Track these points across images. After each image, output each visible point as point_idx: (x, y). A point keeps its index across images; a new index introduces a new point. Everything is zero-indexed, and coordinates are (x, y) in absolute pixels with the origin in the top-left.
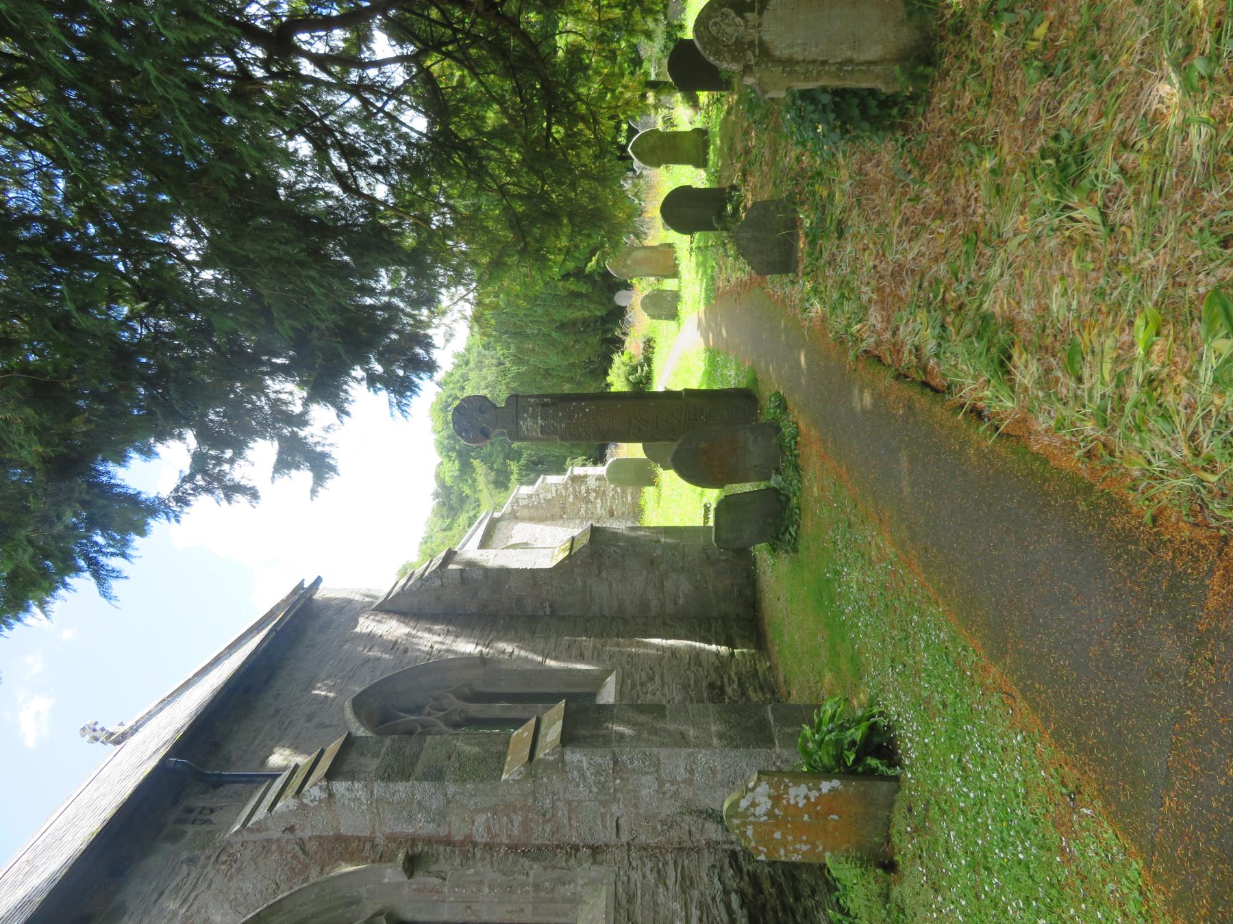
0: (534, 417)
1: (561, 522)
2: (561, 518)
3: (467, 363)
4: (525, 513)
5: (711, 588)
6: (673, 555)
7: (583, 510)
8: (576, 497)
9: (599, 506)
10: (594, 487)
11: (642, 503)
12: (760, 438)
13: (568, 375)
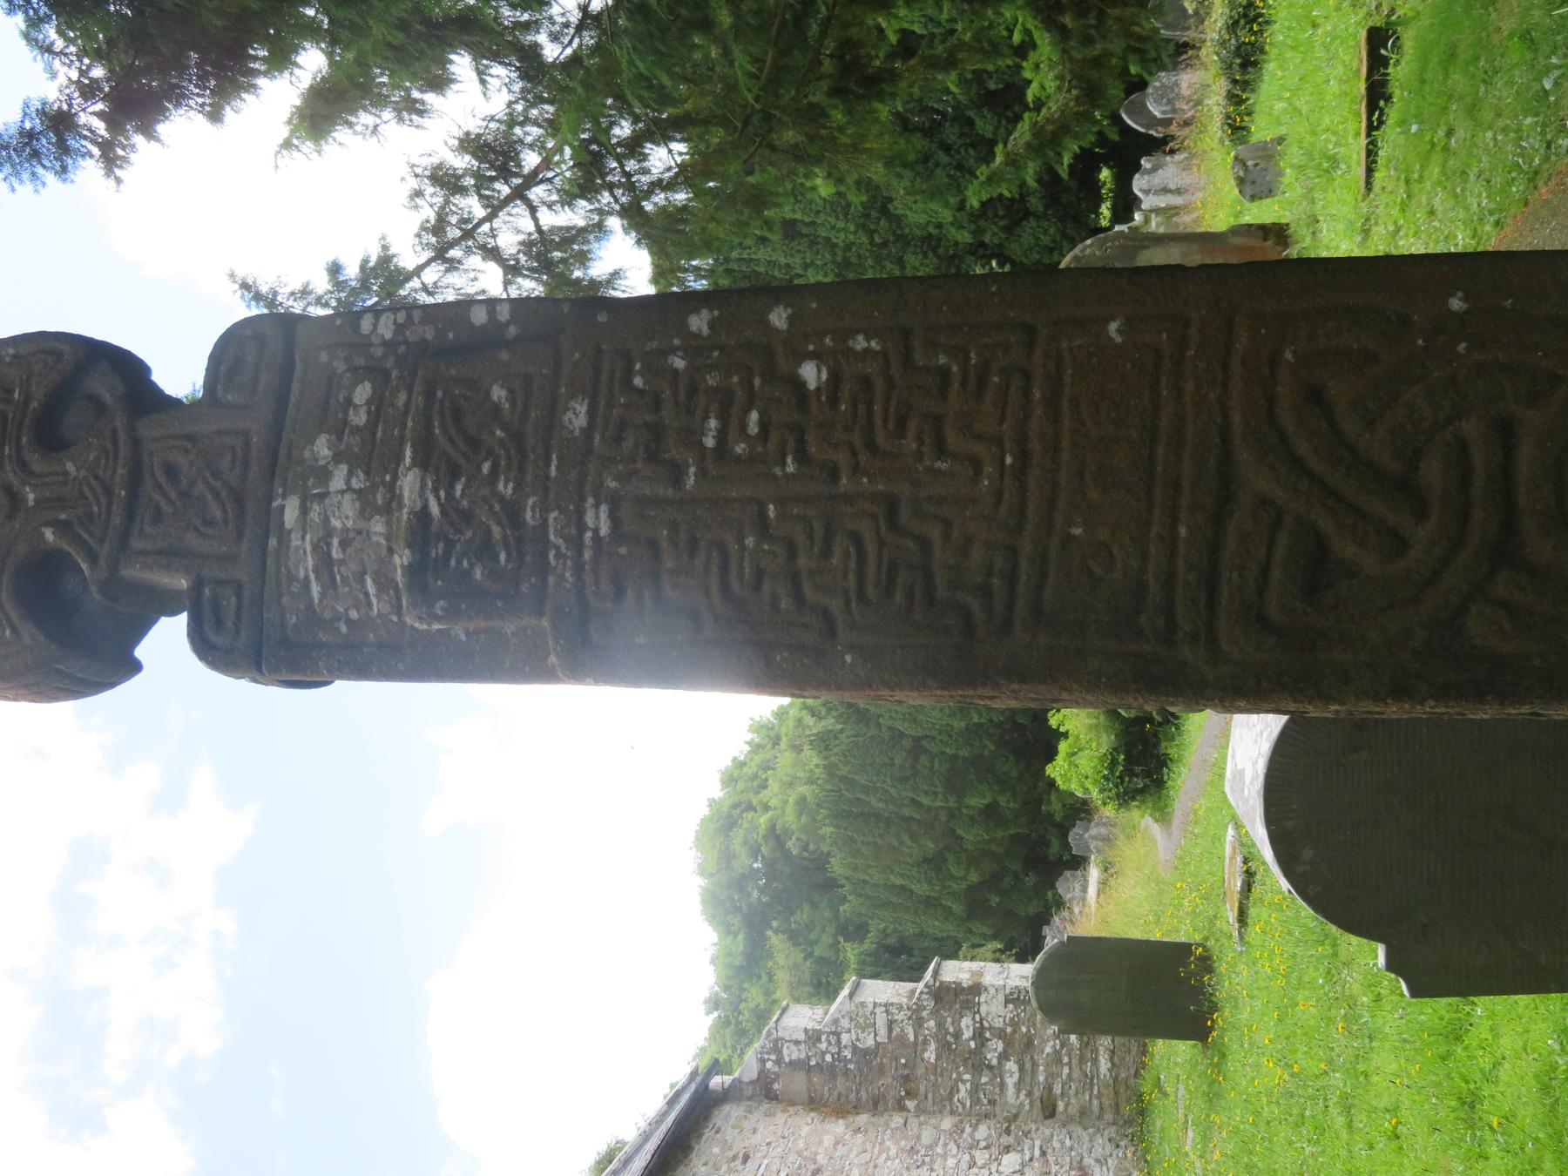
1: (898, 1120)
2: (902, 1108)
3: (776, 741)
4: (798, 1083)
7: (964, 1090)
8: (944, 1047)
9: (1011, 1082)
10: (998, 1023)
13: (964, 753)
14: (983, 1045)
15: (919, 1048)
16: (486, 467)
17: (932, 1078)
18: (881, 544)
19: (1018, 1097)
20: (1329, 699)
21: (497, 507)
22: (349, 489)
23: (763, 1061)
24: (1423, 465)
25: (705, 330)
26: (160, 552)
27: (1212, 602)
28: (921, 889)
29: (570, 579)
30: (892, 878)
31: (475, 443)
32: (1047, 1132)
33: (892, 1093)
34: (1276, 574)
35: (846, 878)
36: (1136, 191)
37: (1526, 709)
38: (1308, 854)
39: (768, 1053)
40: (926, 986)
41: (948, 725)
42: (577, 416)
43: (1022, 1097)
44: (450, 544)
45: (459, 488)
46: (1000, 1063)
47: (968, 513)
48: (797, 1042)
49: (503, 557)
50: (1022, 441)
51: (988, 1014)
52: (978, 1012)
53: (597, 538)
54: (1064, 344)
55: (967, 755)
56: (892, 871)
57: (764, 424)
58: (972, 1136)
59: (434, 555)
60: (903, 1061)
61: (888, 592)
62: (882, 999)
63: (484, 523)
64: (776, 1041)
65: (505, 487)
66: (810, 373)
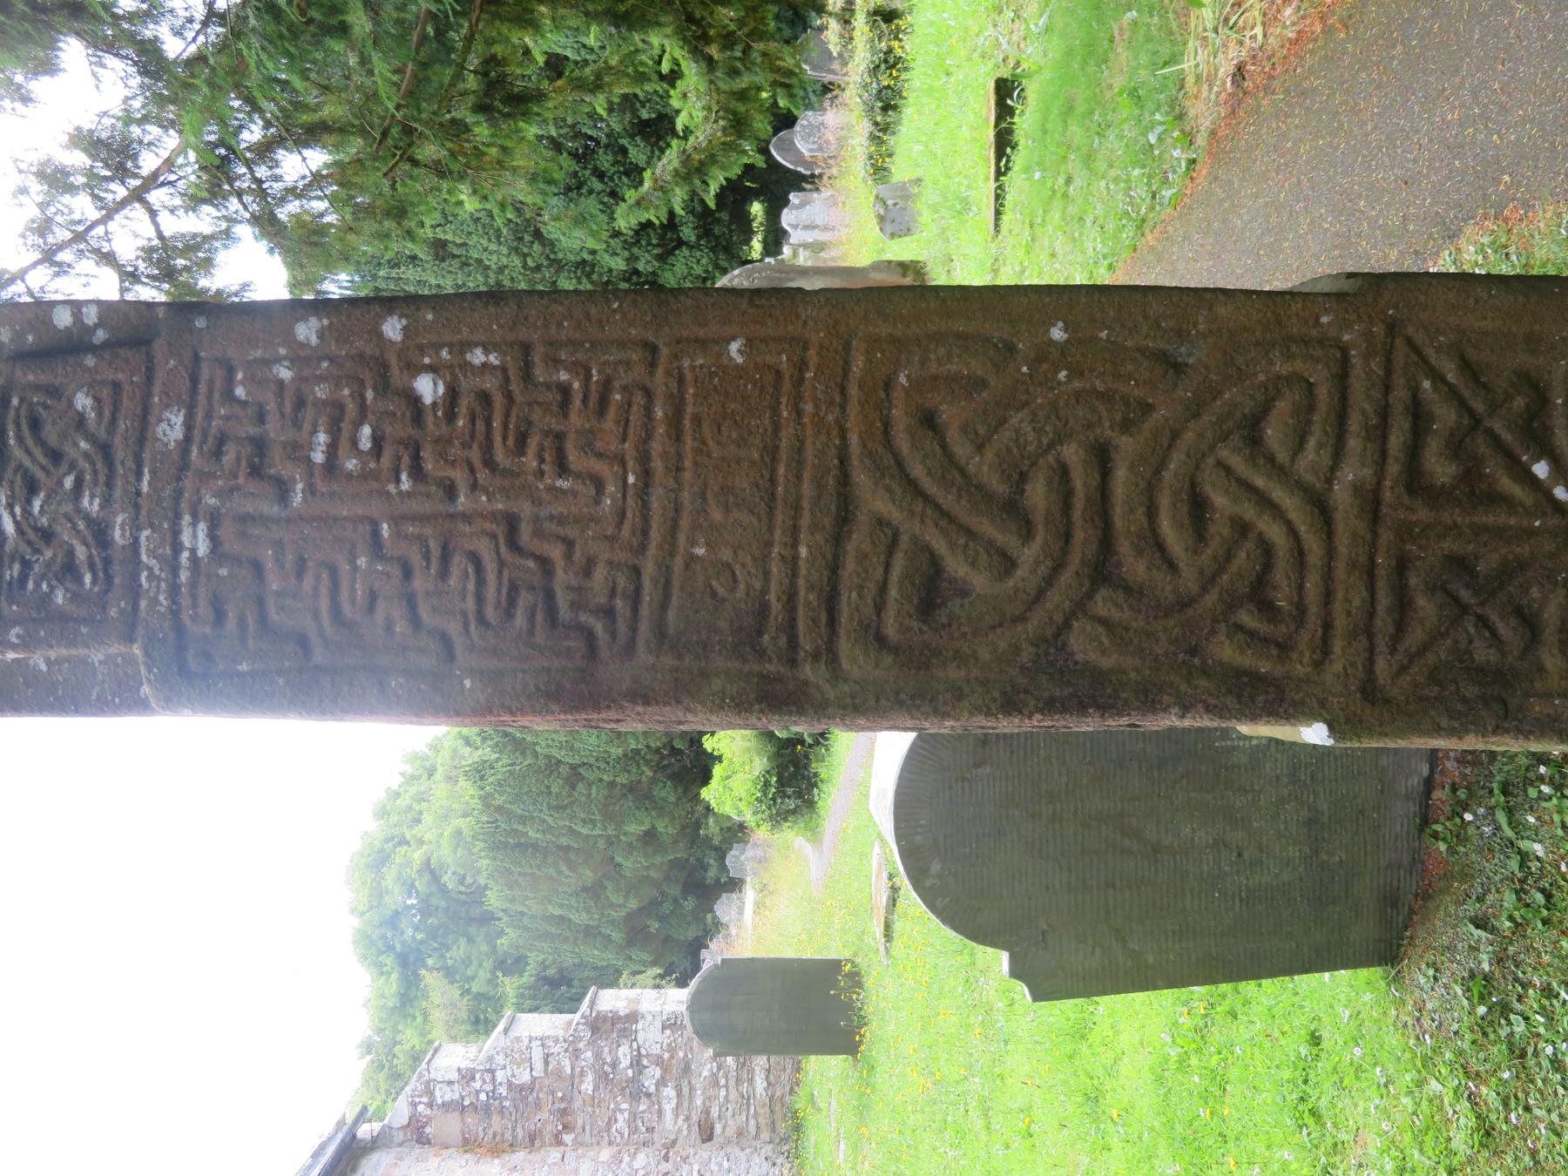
1: (555, 1154)
2: (558, 1142)
3: (431, 772)
4: (450, 1126)
7: (622, 1120)
8: (603, 1078)
9: (668, 1108)
10: (656, 1050)
11: (800, 1103)
13: (622, 779)
14: (641, 1073)
15: (576, 1080)
16: (69, 482)
17: (590, 1109)
18: (502, 564)
19: (676, 1123)
20: (945, 716)
21: (81, 525)
23: (414, 1105)
24: (1028, 487)
25: (314, 340)
27: (832, 622)
28: (580, 918)
29: (165, 603)
30: (550, 907)
31: (56, 456)
32: (706, 1155)
33: (549, 1128)
34: (893, 593)
35: (503, 910)
36: (785, 224)
37: (1124, 721)
38: (936, 867)
39: (420, 1096)
40: (583, 1016)
41: (606, 752)
42: (171, 427)
43: (680, 1122)
44: (26, 565)
45: (37, 505)
46: (657, 1090)
47: (590, 533)
48: (450, 1083)
49: (88, 579)
50: (644, 459)
51: (645, 1041)
52: (635, 1040)
53: (194, 559)
54: (686, 363)
55: (625, 782)
56: (550, 902)
57: (377, 440)
58: (630, 1165)
59: (8, 577)
60: (560, 1095)
61: (509, 614)
62: (538, 1032)
63: (67, 543)
64: (428, 1082)
65: (91, 503)
66: (427, 388)
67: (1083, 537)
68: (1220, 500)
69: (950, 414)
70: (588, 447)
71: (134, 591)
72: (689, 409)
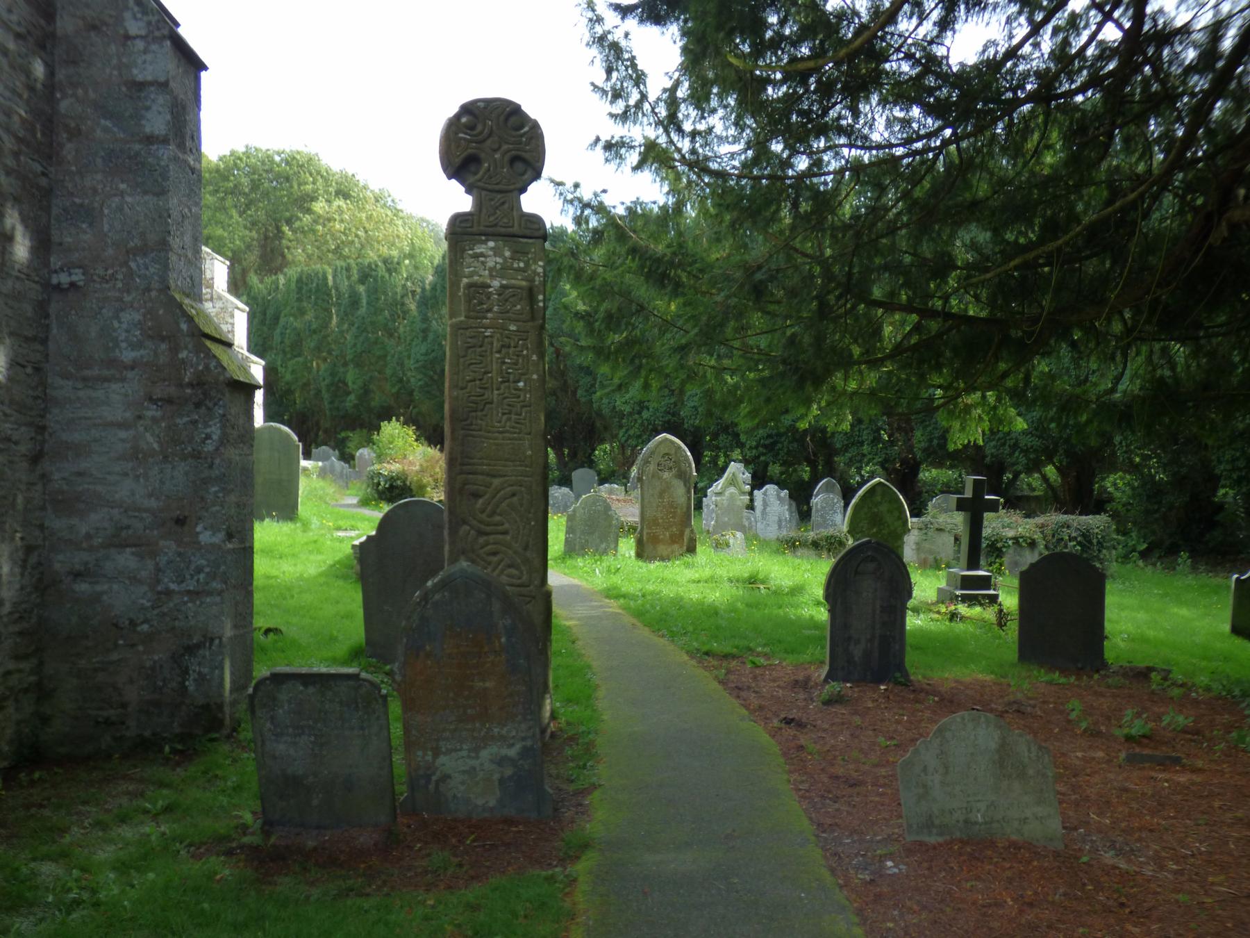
0: (503, 271)
5: (115, 656)
6: (199, 570)
12: (509, 772)
22: (496, 263)
26: (481, 203)
36: (767, 486)
42: (513, 328)
57: (509, 373)
66: (521, 384)
67: (488, 529)
68: (495, 559)
69: (515, 499)
70: (509, 419)
71: (477, 318)
72: (516, 442)
